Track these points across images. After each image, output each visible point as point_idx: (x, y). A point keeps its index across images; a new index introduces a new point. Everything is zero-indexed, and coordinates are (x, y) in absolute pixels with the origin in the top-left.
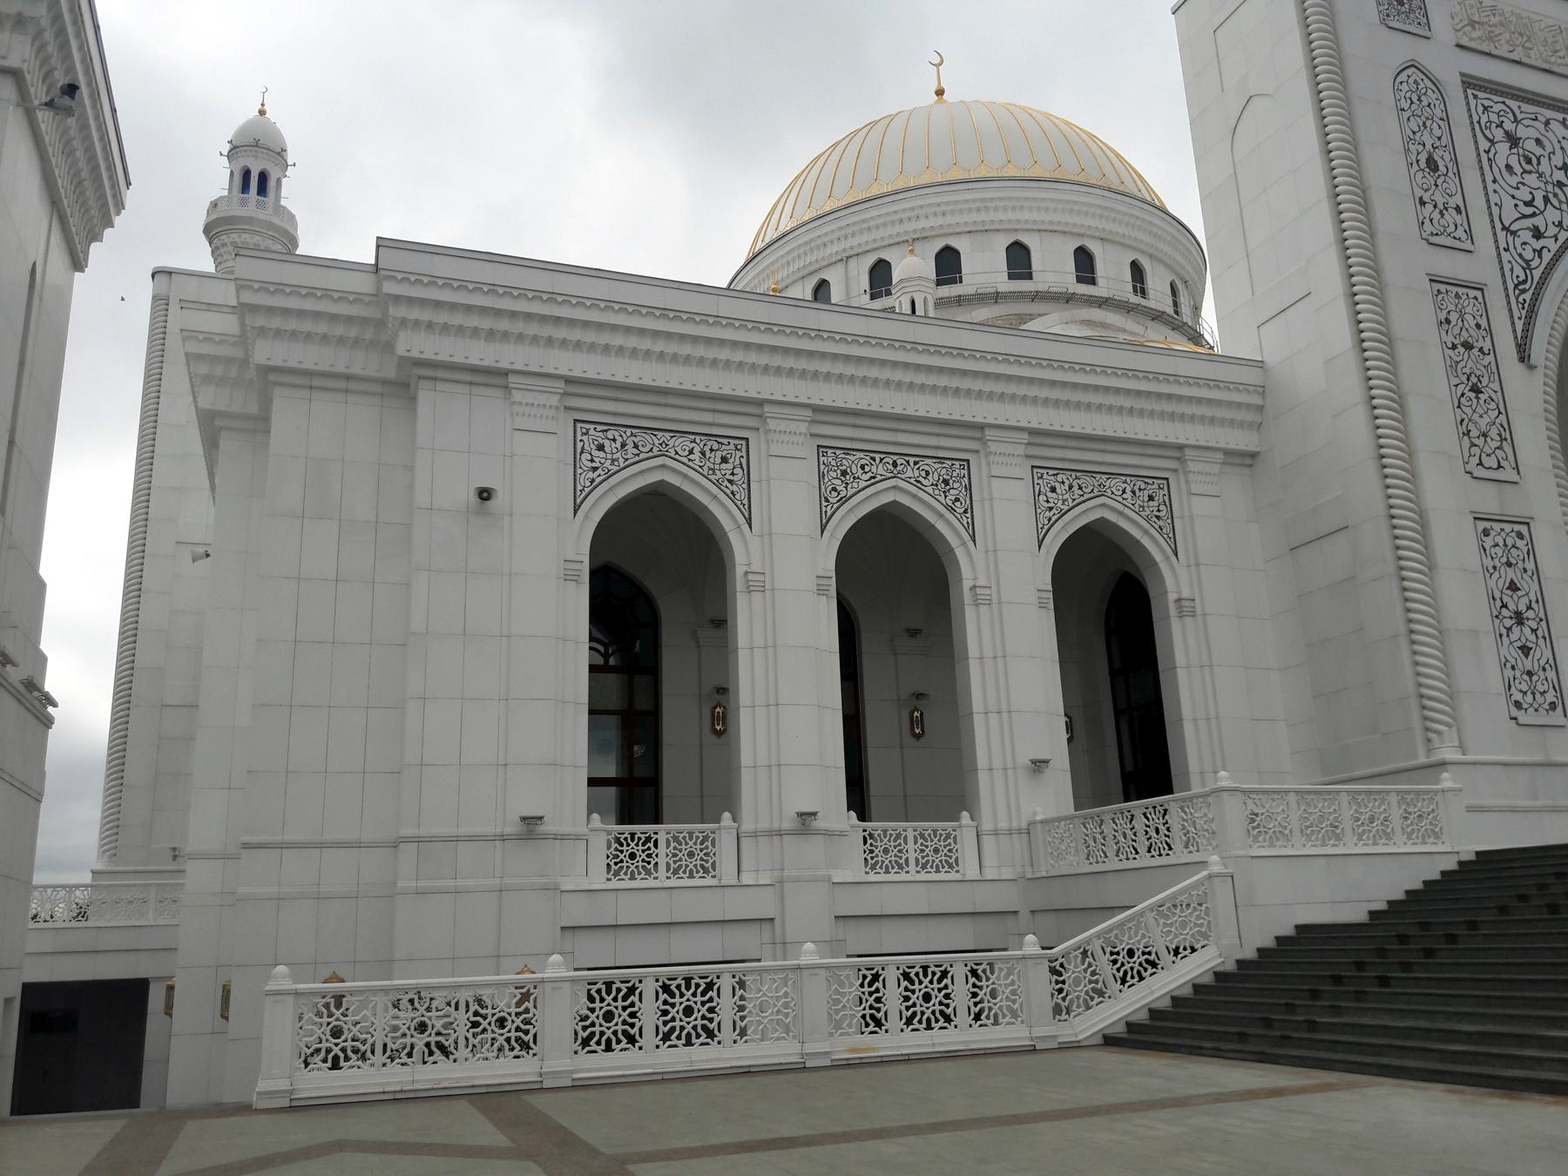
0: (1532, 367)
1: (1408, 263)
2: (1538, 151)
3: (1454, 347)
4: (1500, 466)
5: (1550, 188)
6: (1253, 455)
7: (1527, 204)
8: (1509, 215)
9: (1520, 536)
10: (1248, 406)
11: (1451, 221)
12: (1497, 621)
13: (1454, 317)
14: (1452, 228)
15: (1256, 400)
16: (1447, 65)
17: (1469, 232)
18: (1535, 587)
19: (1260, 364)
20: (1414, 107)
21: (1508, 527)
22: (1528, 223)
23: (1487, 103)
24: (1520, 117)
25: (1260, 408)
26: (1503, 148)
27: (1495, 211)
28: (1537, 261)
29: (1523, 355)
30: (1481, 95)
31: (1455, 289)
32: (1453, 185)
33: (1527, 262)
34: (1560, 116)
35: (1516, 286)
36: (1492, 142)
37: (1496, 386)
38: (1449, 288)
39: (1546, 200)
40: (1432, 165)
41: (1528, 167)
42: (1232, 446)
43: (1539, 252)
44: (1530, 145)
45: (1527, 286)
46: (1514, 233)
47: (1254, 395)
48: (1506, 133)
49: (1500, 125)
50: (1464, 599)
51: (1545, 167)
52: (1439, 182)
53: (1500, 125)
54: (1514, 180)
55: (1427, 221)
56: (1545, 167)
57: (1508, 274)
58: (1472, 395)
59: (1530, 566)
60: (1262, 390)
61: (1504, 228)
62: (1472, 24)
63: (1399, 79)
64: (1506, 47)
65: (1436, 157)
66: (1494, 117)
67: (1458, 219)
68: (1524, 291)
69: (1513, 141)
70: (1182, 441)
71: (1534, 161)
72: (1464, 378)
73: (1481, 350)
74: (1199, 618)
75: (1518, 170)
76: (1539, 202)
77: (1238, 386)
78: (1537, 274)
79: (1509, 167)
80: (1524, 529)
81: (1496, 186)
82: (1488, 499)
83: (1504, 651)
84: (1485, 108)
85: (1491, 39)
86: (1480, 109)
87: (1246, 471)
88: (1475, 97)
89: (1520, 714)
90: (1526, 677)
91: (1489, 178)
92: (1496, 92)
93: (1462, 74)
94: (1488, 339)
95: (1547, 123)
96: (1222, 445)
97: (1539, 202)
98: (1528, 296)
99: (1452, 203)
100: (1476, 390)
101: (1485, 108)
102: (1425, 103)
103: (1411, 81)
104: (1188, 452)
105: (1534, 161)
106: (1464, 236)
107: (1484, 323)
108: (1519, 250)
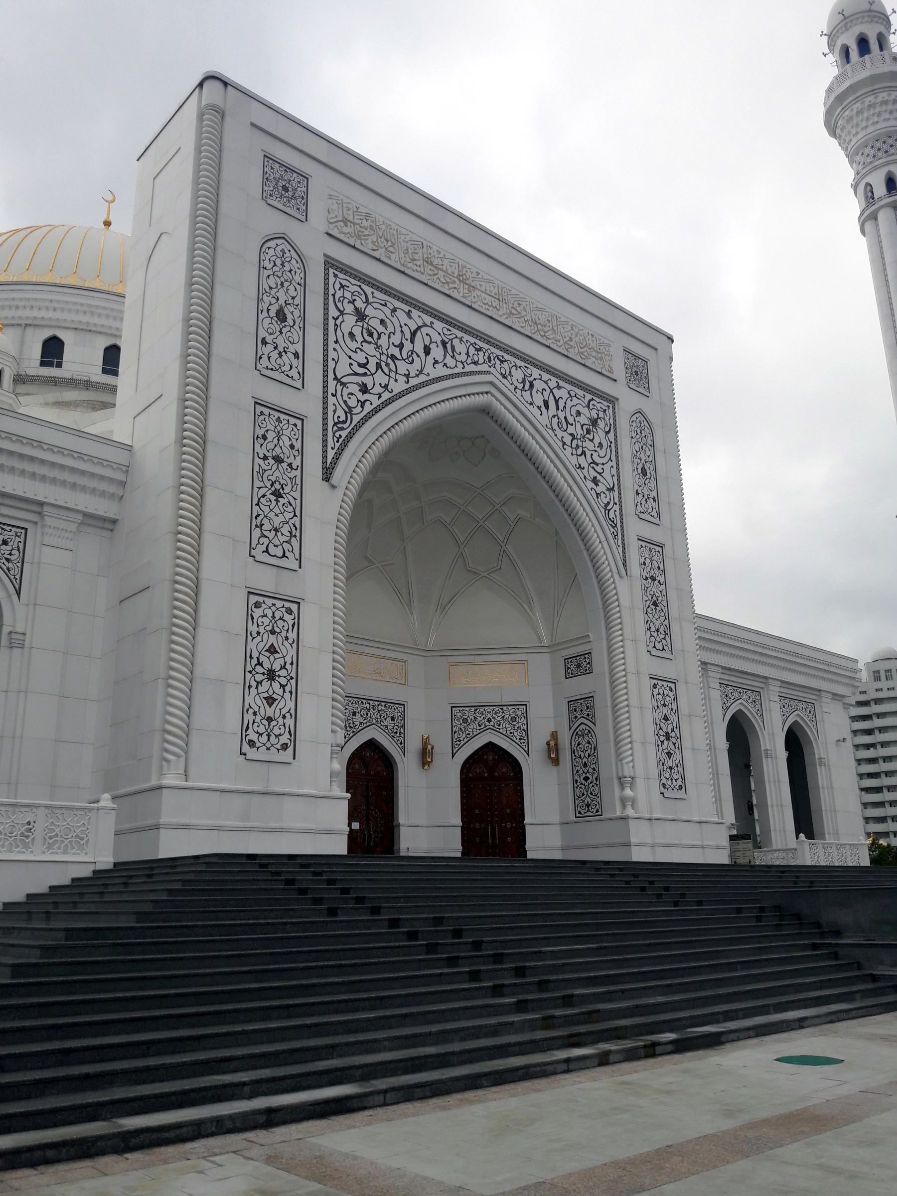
0: (333, 487)
1: (237, 384)
2: (381, 329)
3: (265, 458)
4: (284, 556)
5: (384, 358)
6: (114, 522)
7: (360, 365)
8: (343, 369)
9: (289, 611)
10: (112, 480)
11: (287, 362)
12: (249, 675)
13: (271, 435)
14: (287, 367)
15: (120, 476)
16: (314, 244)
17: (302, 375)
18: (293, 652)
19: (129, 448)
20: (275, 269)
21: (279, 604)
23: (344, 283)
24: (371, 300)
25: (123, 484)
26: (350, 321)
27: (331, 364)
28: (359, 409)
29: (327, 474)
30: (340, 275)
31: (277, 414)
32: (296, 335)
33: (350, 408)
34: (407, 308)
35: (335, 424)
36: (342, 313)
37: (297, 495)
38: (272, 412)
39: (378, 366)
40: (281, 316)
41: (369, 339)
42: (91, 510)
43: (363, 404)
44: (375, 323)
45: (345, 426)
46: (344, 384)
47: (118, 474)
48: (356, 309)
49: (353, 302)
50: (221, 652)
51: (384, 341)
52: (284, 330)
53: (353, 302)
54: (353, 345)
55: (265, 358)
56: (384, 341)
57: (330, 413)
58: (273, 498)
59: (292, 635)
60: (127, 469)
61: (336, 378)
62: (345, 221)
63: (272, 244)
64: (370, 246)
65: (286, 311)
66: (348, 295)
67: (295, 362)
68: (342, 429)
69: (361, 316)
70: (42, 499)
71: (375, 336)
72: (268, 484)
73: (290, 465)
74: (26, 650)
75: (359, 338)
76: (372, 367)
77: (110, 464)
78: (356, 419)
79: (351, 335)
80: (294, 607)
81: (337, 346)
82: (265, 579)
83: (249, 700)
84: (342, 286)
85: (359, 237)
86: (337, 286)
87: (106, 533)
88: (336, 276)
89: (252, 753)
90: (266, 722)
91: (332, 338)
92: (355, 277)
93: (325, 255)
94: (299, 458)
95: (394, 310)
96: (81, 508)
97: (372, 367)
98: (344, 434)
99: (292, 348)
100: (278, 495)
101: (342, 286)
102: (287, 268)
103: (279, 249)
104: (46, 508)
105: (375, 336)
106: (296, 376)
107: (298, 445)
108: (345, 398)
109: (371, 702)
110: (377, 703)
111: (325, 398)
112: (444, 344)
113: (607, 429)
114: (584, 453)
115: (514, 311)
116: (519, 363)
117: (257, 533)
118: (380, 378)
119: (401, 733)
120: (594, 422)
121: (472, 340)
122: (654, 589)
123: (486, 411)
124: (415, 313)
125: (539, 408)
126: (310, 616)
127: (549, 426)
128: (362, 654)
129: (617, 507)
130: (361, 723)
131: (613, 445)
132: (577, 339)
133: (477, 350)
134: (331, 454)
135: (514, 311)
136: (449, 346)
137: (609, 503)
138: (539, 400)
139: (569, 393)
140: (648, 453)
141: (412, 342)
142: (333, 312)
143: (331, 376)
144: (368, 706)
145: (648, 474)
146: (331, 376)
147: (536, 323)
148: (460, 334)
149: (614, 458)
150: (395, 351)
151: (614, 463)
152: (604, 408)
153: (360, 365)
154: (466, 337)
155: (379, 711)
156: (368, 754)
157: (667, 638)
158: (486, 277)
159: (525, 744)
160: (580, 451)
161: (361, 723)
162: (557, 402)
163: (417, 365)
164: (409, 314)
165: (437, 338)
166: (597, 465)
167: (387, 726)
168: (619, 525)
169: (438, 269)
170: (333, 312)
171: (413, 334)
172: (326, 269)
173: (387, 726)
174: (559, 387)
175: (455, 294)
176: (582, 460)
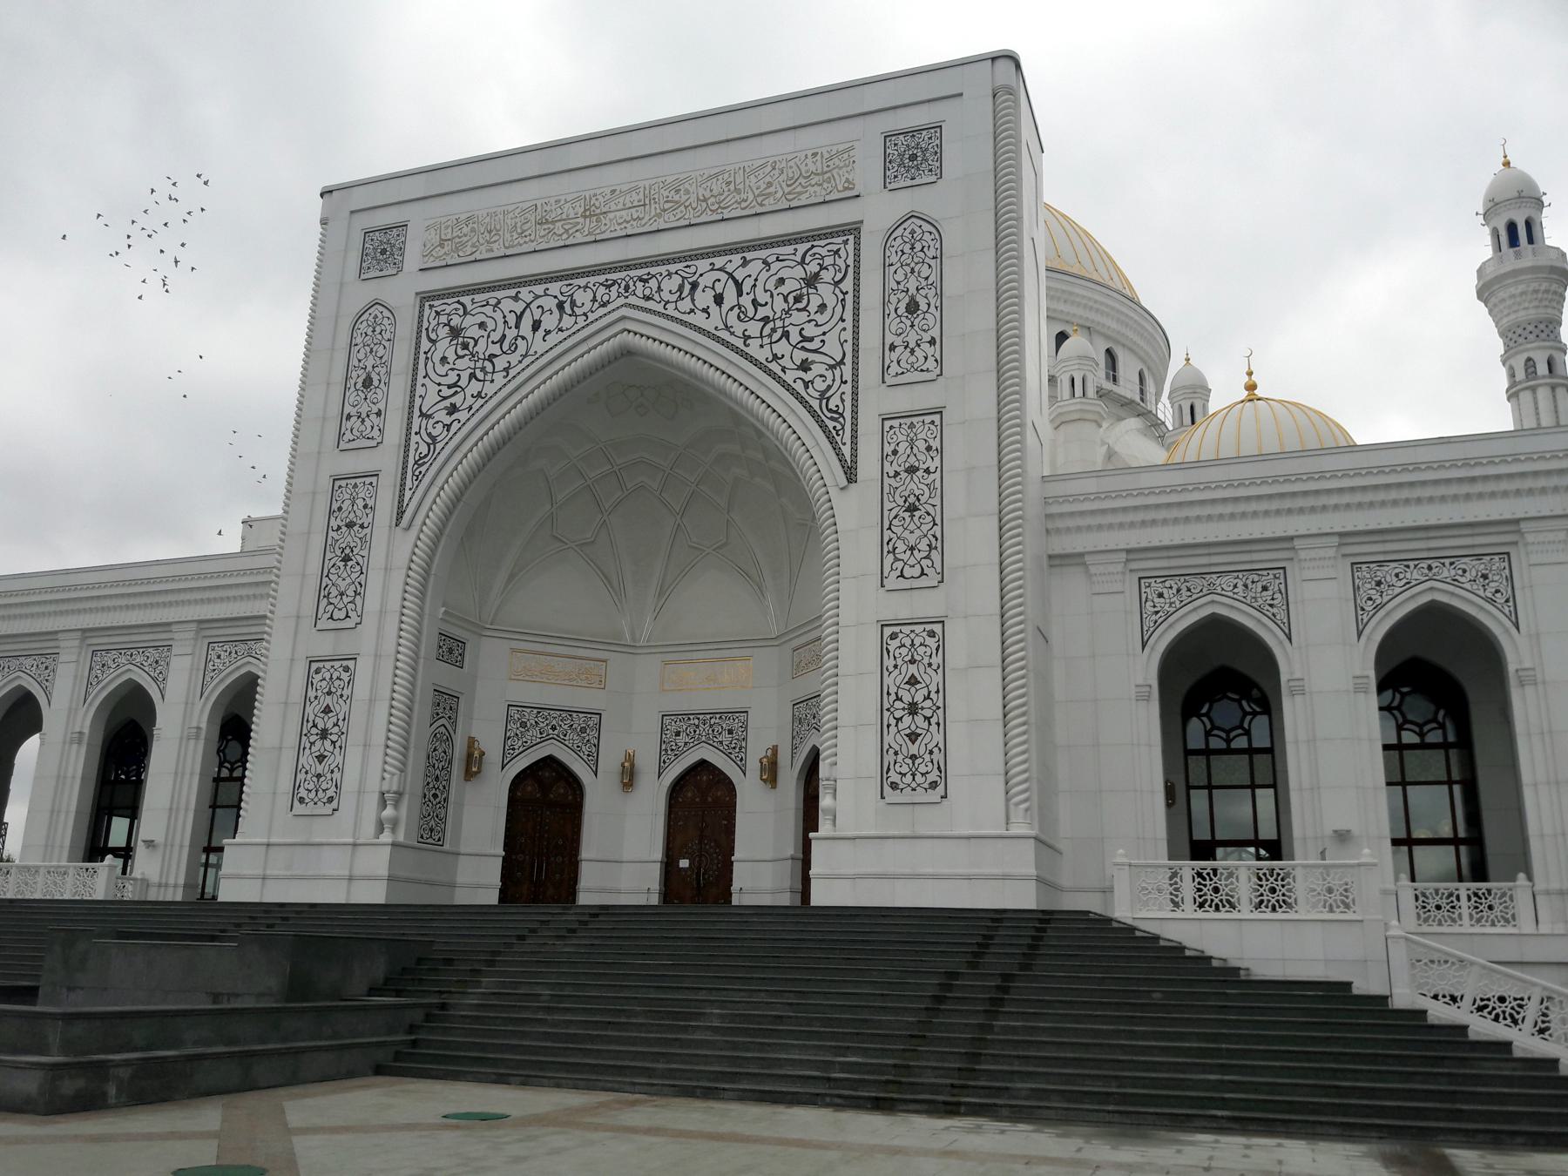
7: (450, 387)
22: (447, 403)
24: (469, 308)
26: (445, 347)
27: (418, 401)
30: (436, 303)
33: (433, 438)
34: (512, 292)
39: (473, 376)
43: (448, 427)
46: (429, 417)
61: (422, 415)
64: (469, 250)
69: (455, 332)
72: (338, 552)
79: (444, 360)
82: (324, 645)
91: (421, 373)
92: (450, 295)
111: (408, 440)
112: (560, 306)
113: (839, 276)
114: (786, 335)
115: (667, 206)
116: (673, 268)
117: (324, 602)
118: (475, 387)
120: (812, 281)
121: (601, 278)
122: (912, 486)
123: (627, 353)
124: (525, 294)
125: (705, 310)
126: (363, 669)
127: (721, 326)
128: (691, 661)
129: (847, 388)
131: (849, 299)
132: (784, 177)
133: (608, 287)
134: (408, 494)
135: (667, 206)
136: (567, 306)
137: (829, 387)
138: (704, 298)
139: (765, 262)
140: (925, 271)
141: (517, 327)
142: (425, 345)
143: (417, 413)
145: (923, 307)
146: (417, 413)
147: (705, 200)
148: (582, 282)
149: (848, 316)
150: (495, 349)
151: (849, 324)
152: (835, 248)
153: (450, 387)
154: (592, 280)
157: (935, 555)
158: (625, 188)
159: (737, 750)
160: (776, 336)
162: (739, 286)
163: (522, 349)
164: (516, 298)
165: (550, 303)
166: (811, 339)
168: (848, 414)
169: (553, 222)
170: (425, 345)
171: (519, 318)
172: (422, 307)
174: (745, 263)
175: (579, 238)
176: (782, 348)
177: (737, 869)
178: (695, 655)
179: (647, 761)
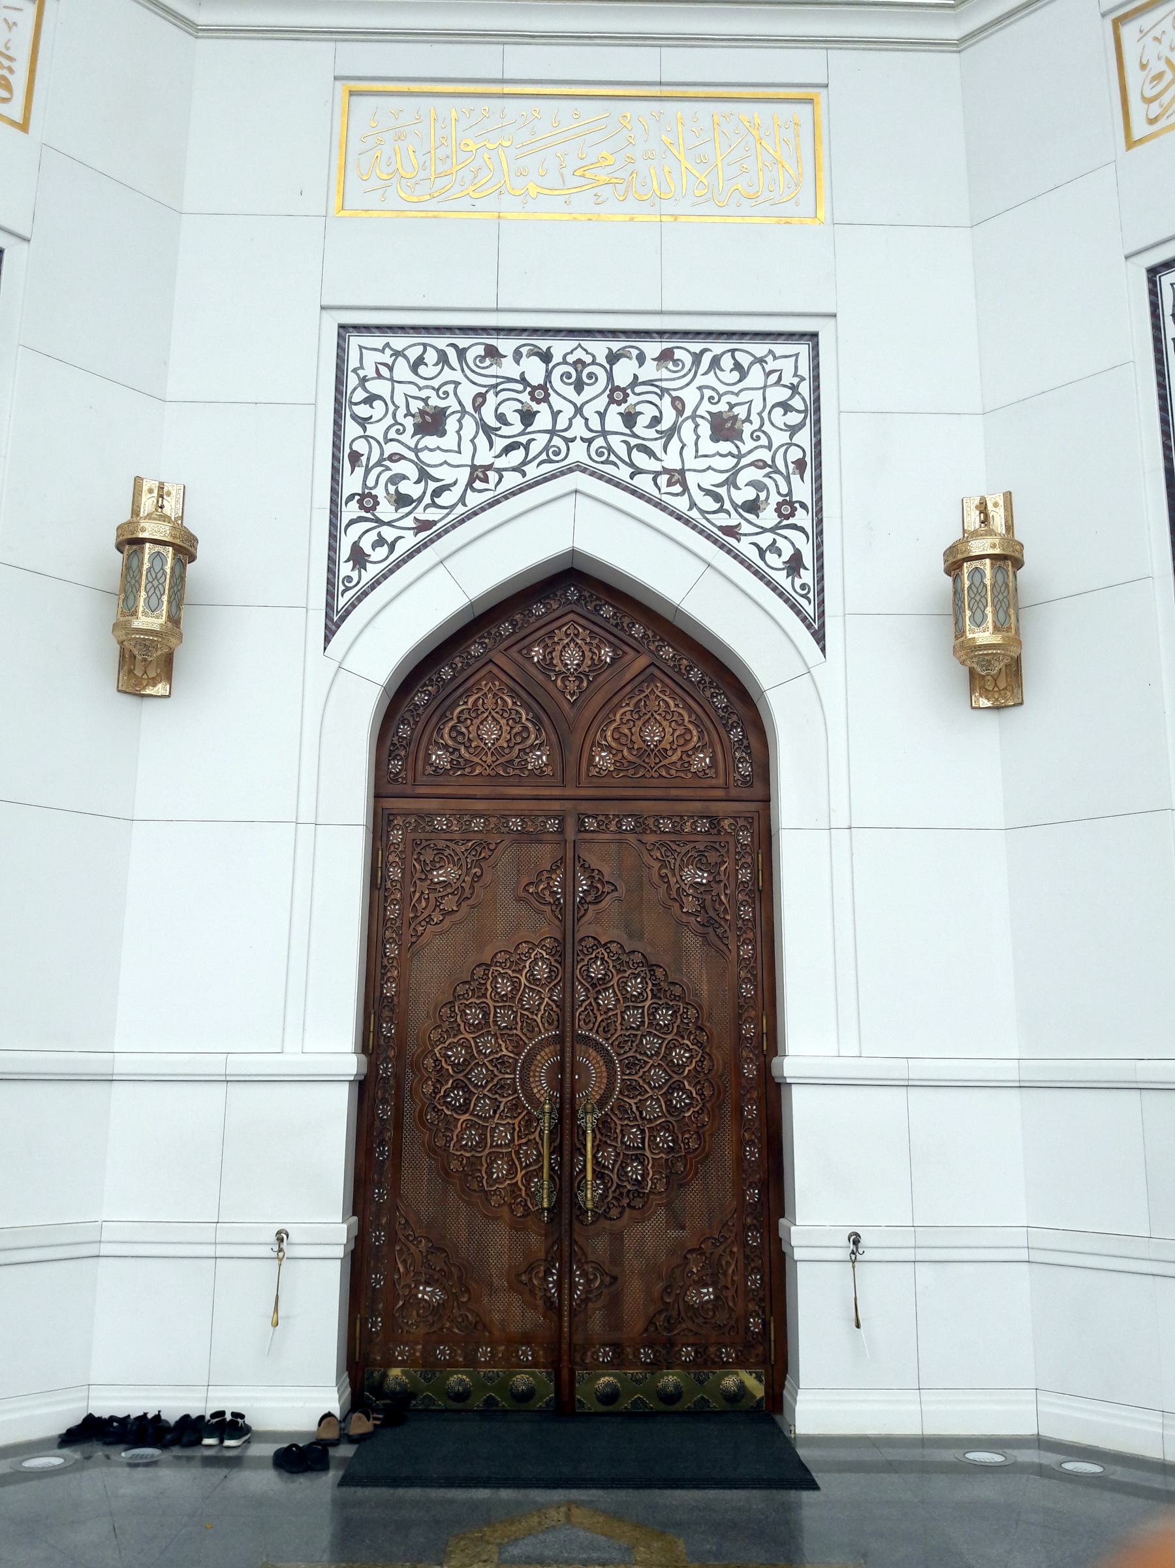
109: (559, 348)
110: (600, 348)
119: (787, 507)
128: (498, 88)
130: (478, 473)
144: (535, 371)
155: (616, 394)
156: (572, 658)
161: (478, 473)
167: (678, 477)
173: (678, 477)
177: (810, 1122)
178: (523, 61)
179: (261, 535)
